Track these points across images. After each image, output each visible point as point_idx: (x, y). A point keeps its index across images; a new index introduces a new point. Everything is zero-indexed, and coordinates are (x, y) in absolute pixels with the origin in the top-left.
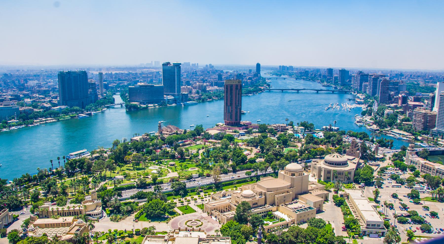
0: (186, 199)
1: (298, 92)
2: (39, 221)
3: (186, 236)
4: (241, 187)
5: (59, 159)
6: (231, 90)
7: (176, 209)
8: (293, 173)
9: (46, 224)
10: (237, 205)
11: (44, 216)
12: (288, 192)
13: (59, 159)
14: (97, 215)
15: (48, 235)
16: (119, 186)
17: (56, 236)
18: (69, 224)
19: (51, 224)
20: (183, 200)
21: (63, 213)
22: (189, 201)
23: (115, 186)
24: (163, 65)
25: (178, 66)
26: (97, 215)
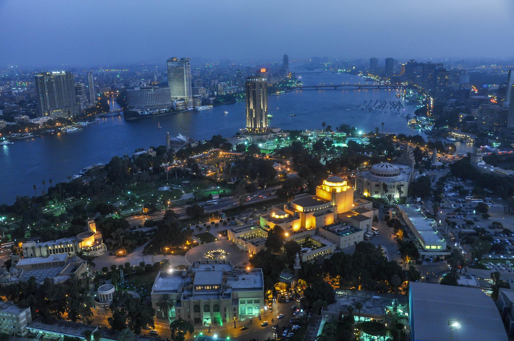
0: (205, 225)
1: (335, 89)
2: (22, 262)
3: (208, 270)
9: (32, 265)
15: (36, 278)
17: (47, 278)
19: (39, 264)
21: (53, 250)
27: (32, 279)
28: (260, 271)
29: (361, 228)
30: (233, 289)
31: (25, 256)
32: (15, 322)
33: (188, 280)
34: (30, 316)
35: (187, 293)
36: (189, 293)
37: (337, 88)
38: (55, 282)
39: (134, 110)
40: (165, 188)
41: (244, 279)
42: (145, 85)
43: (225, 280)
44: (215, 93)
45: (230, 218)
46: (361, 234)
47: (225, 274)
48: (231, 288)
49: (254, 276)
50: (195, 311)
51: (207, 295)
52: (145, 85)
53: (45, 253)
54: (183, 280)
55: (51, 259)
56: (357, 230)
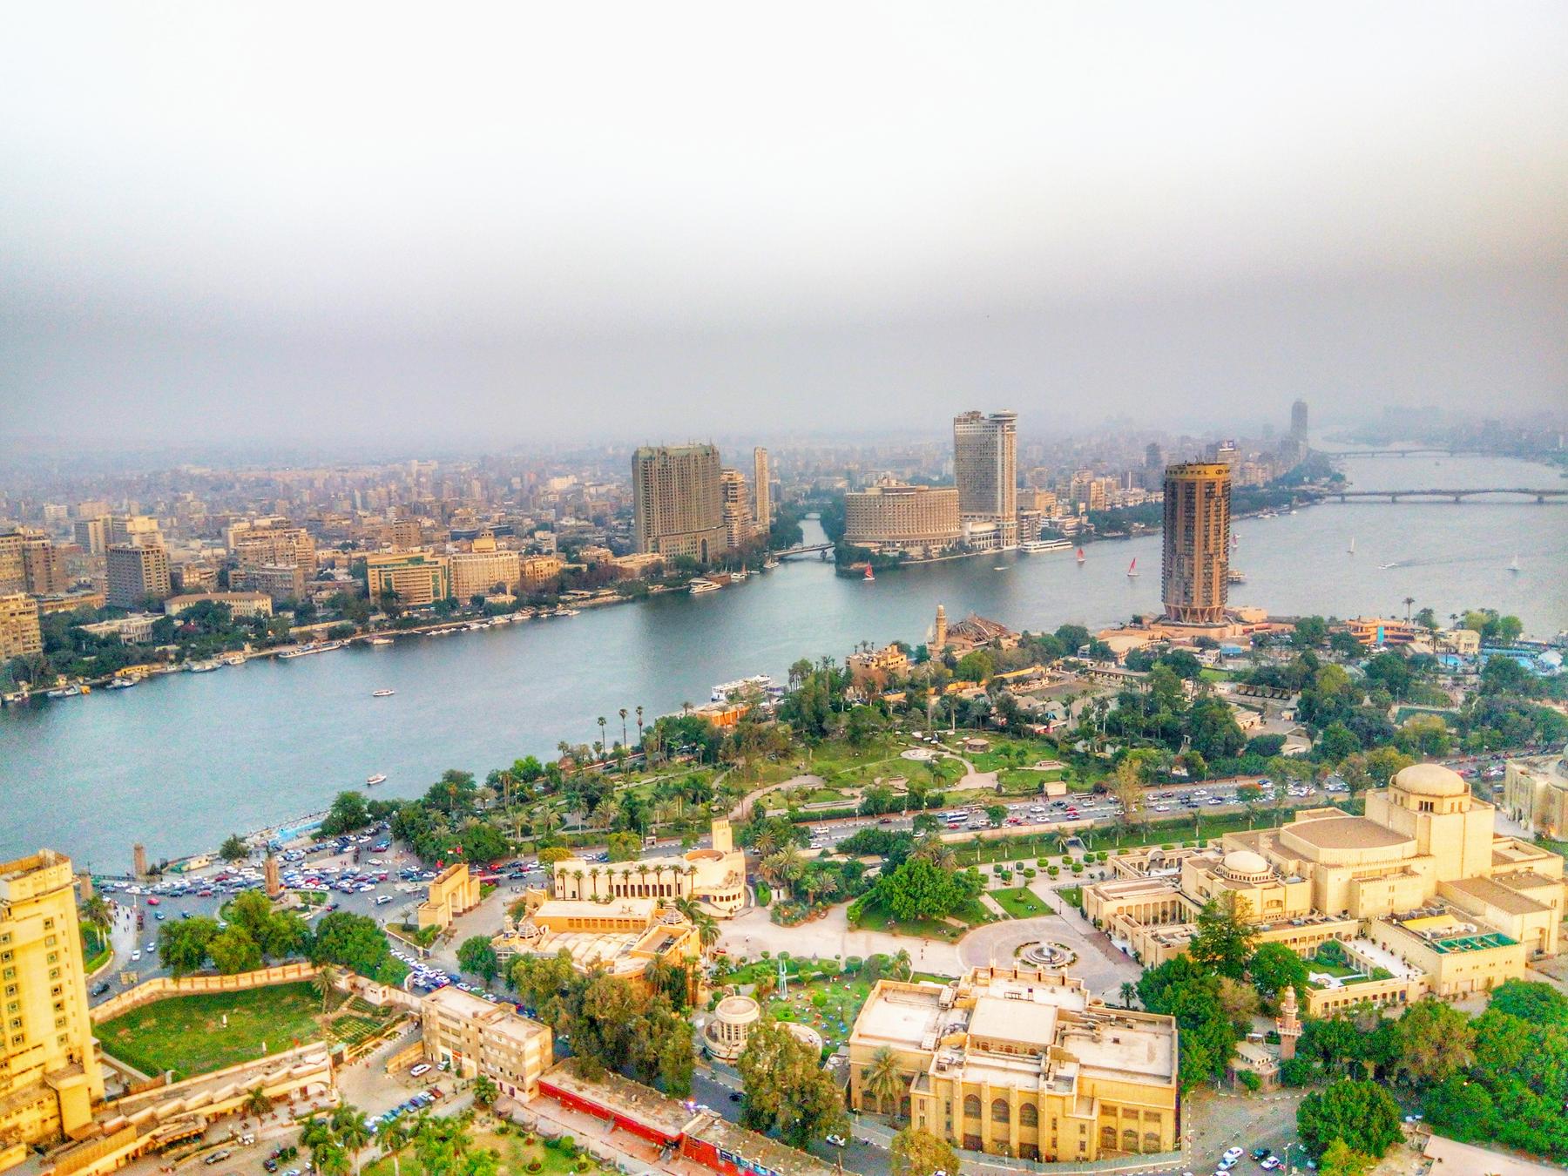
0: (1020, 867)
1: (1457, 502)
4: (1218, 840)
5: (623, 713)
6: (1190, 496)
7: (987, 901)
8: (1425, 799)
10: (1204, 902)
11: (569, 895)
12: (1405, 871)
13: (623, 713)
14: (728, 899)
16: (801, 810)
18: (639, 925)
20: (1009, 866)
22: (1029, 874)
23: (792, 809)
24: (958, 421)
25: (1000, 420)
26: (728, 899)
27: (565, 954)
28: (1169, 1024)
29: (1516, 937)
30: (1083, 1066)
31: (559, 894)
32: (514, 1060)
33: (956, 1017)
34: (549, 1051)
35: (949, 1056)
36: (957, 1058)
37: (1463, 498)
38: (618, 972)
39: (861, 545)
40: (923, 754)
41: (1116, 1041)
42: (893, 483)
43: (1061, 1036)
44: (1082, 505)
45: (1095, 854)
46: (1519, 954)
47: (1062, 1015)
48: (1077, 1061)
49: (1149, 1037)
50: (967, 1114)
51: (1005, 1070)
52: (893, 483)
53: (603, 892)
54: (943, 1015)
55: (614, 910)
56: (1502, 940)
